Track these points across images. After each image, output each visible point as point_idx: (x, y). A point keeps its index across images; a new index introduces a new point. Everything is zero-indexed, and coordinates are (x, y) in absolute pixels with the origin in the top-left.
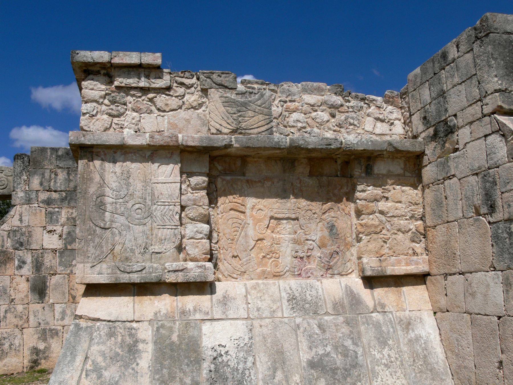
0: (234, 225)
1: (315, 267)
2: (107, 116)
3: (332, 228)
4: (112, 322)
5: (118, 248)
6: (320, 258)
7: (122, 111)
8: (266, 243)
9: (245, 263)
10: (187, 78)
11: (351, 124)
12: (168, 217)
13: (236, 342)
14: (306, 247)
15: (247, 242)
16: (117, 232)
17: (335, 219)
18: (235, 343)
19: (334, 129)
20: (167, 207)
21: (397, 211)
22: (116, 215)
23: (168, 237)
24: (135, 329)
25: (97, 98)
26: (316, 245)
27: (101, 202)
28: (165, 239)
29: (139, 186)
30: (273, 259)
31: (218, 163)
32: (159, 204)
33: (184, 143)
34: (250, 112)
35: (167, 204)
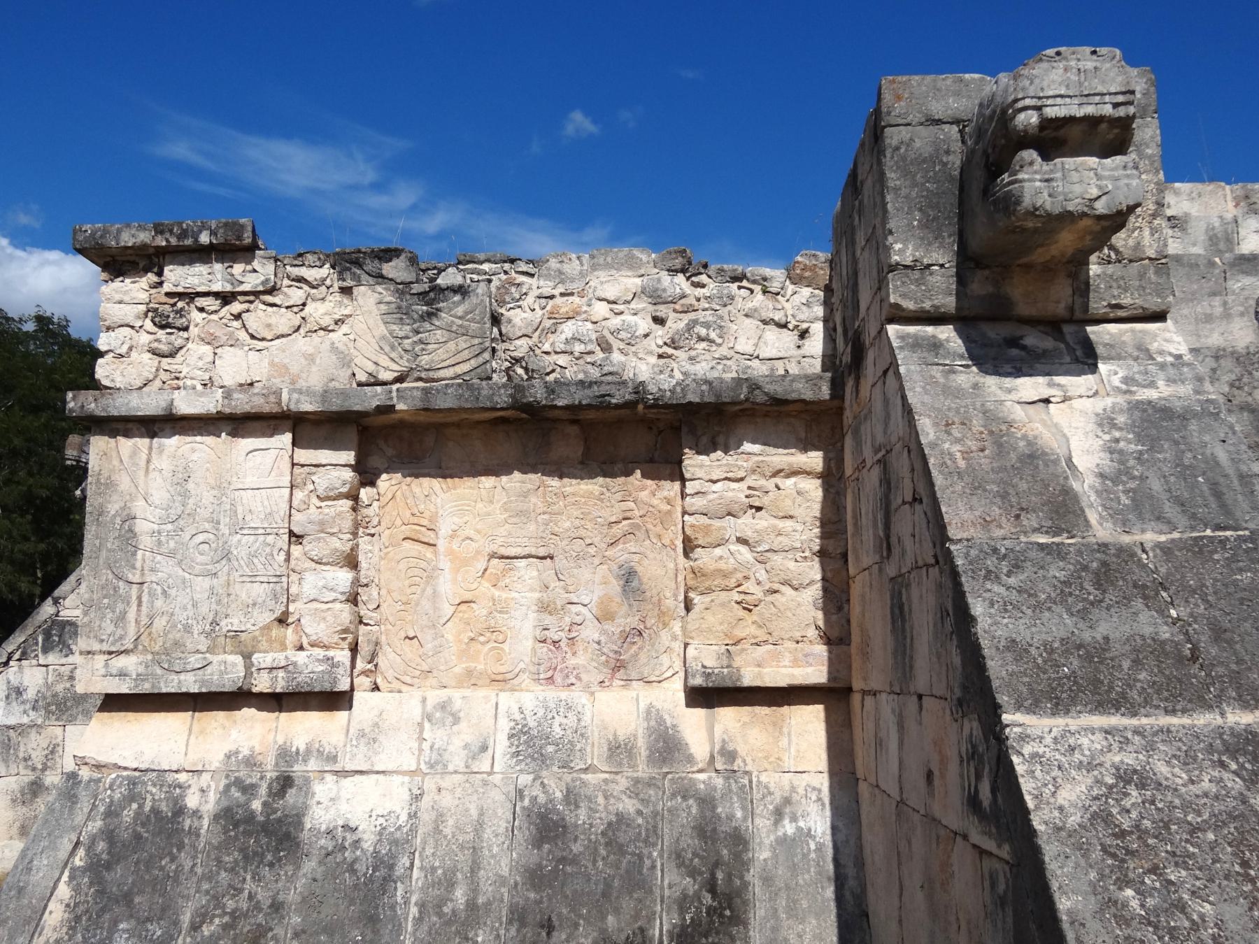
2: (150, 355)
3: (629, 576)
5: (160, 623)
6: (599, 643)
7: (179, 343)
8: (480, 610)
13: (381, 820)
14: (567, 620)
15: (436, 609)
18: (378, 823)
19: (661, 351)
20: (261, 538)
21: (780, 538)
22: (159, 557)
23: (260, 600)
24: (181, 787)
25: (130, 319)
27: (131, 530)
28: (254, 605)
29: (208, 497)
33: (293, 407)
34: (439, 332)
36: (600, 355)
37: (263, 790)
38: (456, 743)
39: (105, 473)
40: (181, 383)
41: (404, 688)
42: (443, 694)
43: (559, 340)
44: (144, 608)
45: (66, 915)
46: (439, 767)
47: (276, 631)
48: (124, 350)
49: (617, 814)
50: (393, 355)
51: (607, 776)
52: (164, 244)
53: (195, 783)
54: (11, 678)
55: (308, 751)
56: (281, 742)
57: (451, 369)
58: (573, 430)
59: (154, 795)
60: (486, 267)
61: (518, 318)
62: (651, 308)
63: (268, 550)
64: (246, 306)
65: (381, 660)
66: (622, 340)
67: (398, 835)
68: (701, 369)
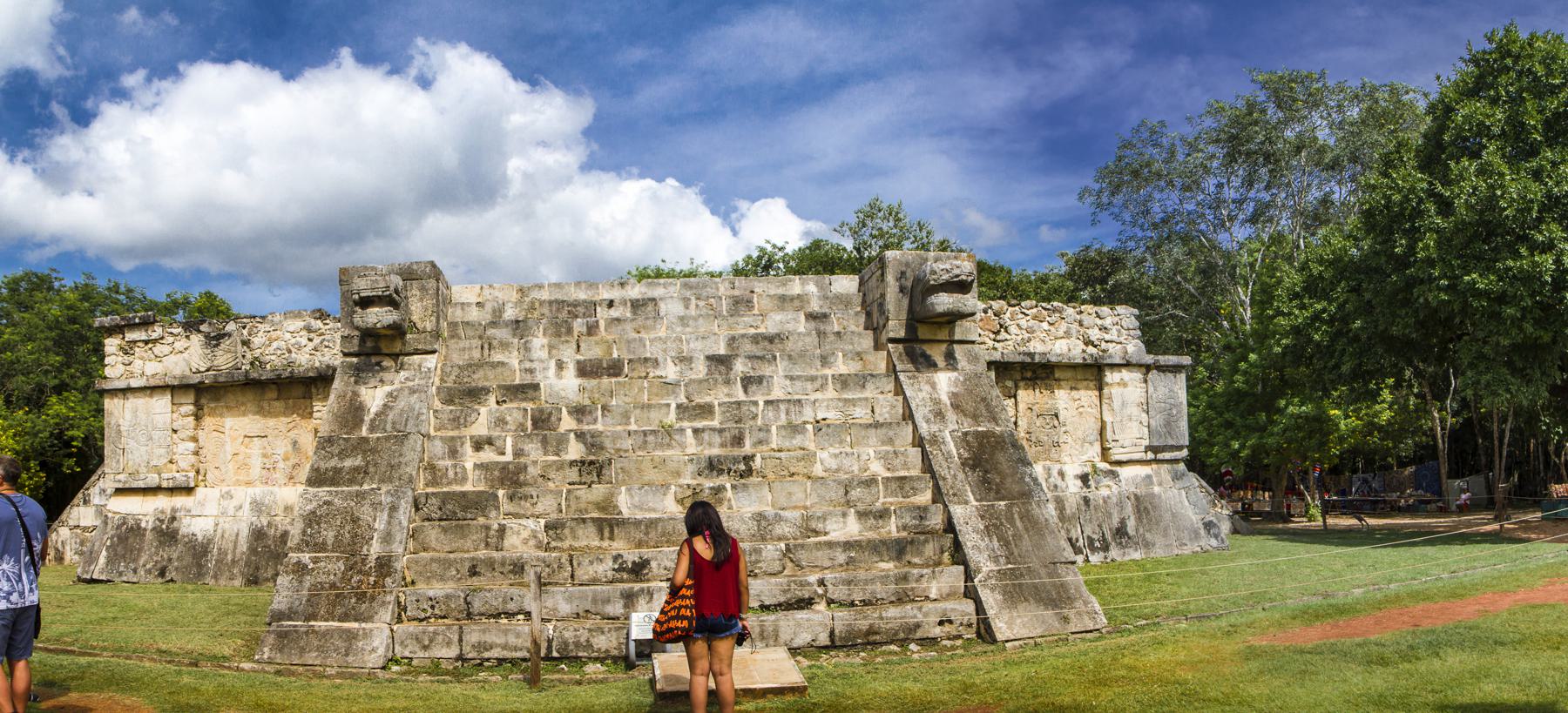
3: (295, 443)
8: (240, 457)
43: (271, 349)
53: (144, 519)
59: (131, 522)
61: (257, 341)
68: (326, 359)
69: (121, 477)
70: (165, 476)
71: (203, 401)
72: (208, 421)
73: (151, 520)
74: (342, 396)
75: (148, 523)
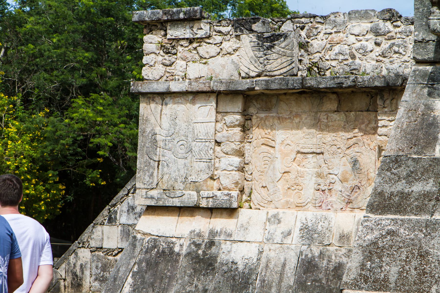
0: (264, 159)
1: (335, 200)
3: (355, 162)
4: (159, 237)
5: (166, 177)
6: (341, 191)
7: (173, 60)
8: (292, 176)
9: (272, 194)
10: (224, 26)
11: (396, 53)
12: (204, 152)
13: (246, 261)
14: (328, 181)
15: (274, 175)
16: (165, 164)
17: (359, 154)
18: (245, 262)
19: (378, 58)
20: (204, 143)
22: (165, 151)
24: (173, 243)
26: (338, 180)
27: (155, 139)
28: (201, 171)
29: (184, 125)
30: (297, 191)
31: (256, 101)
32: (198, 140)
34: (274, 55)
35: (204, 140)
36: (350, 61)
37: (203, 246)
38: (278, 231)
39: (145, 115)
40: (174, 77)
41: (261, 208)
42: (275, 211)
43: (331, 54)
44: (160, 171)
45: (131, 289)
46: (271, 241)
47: (210, 182)
48: (152, 63)
49: (339, 264)
50: (256, 65)
51: (337, 248)
52: (166, 19)
53: (178, 242)
54: (130, 202)
55: (221, 232)
56: (211, 228)
57: (279, 71)
58: (334, 97)
60: (303, 20)
61: (316, 44)
62: (374, 38)
63: (206, 148)
64: (198, 44)
65: (252, 196)
66: (360, 54)
67: (252, 267)
69: (154, 193)
70: (204, 193)
71: (252, 110)
72: (257, 133)
73: (186, 243)
74: (412, 110)
75: (182, 247)
